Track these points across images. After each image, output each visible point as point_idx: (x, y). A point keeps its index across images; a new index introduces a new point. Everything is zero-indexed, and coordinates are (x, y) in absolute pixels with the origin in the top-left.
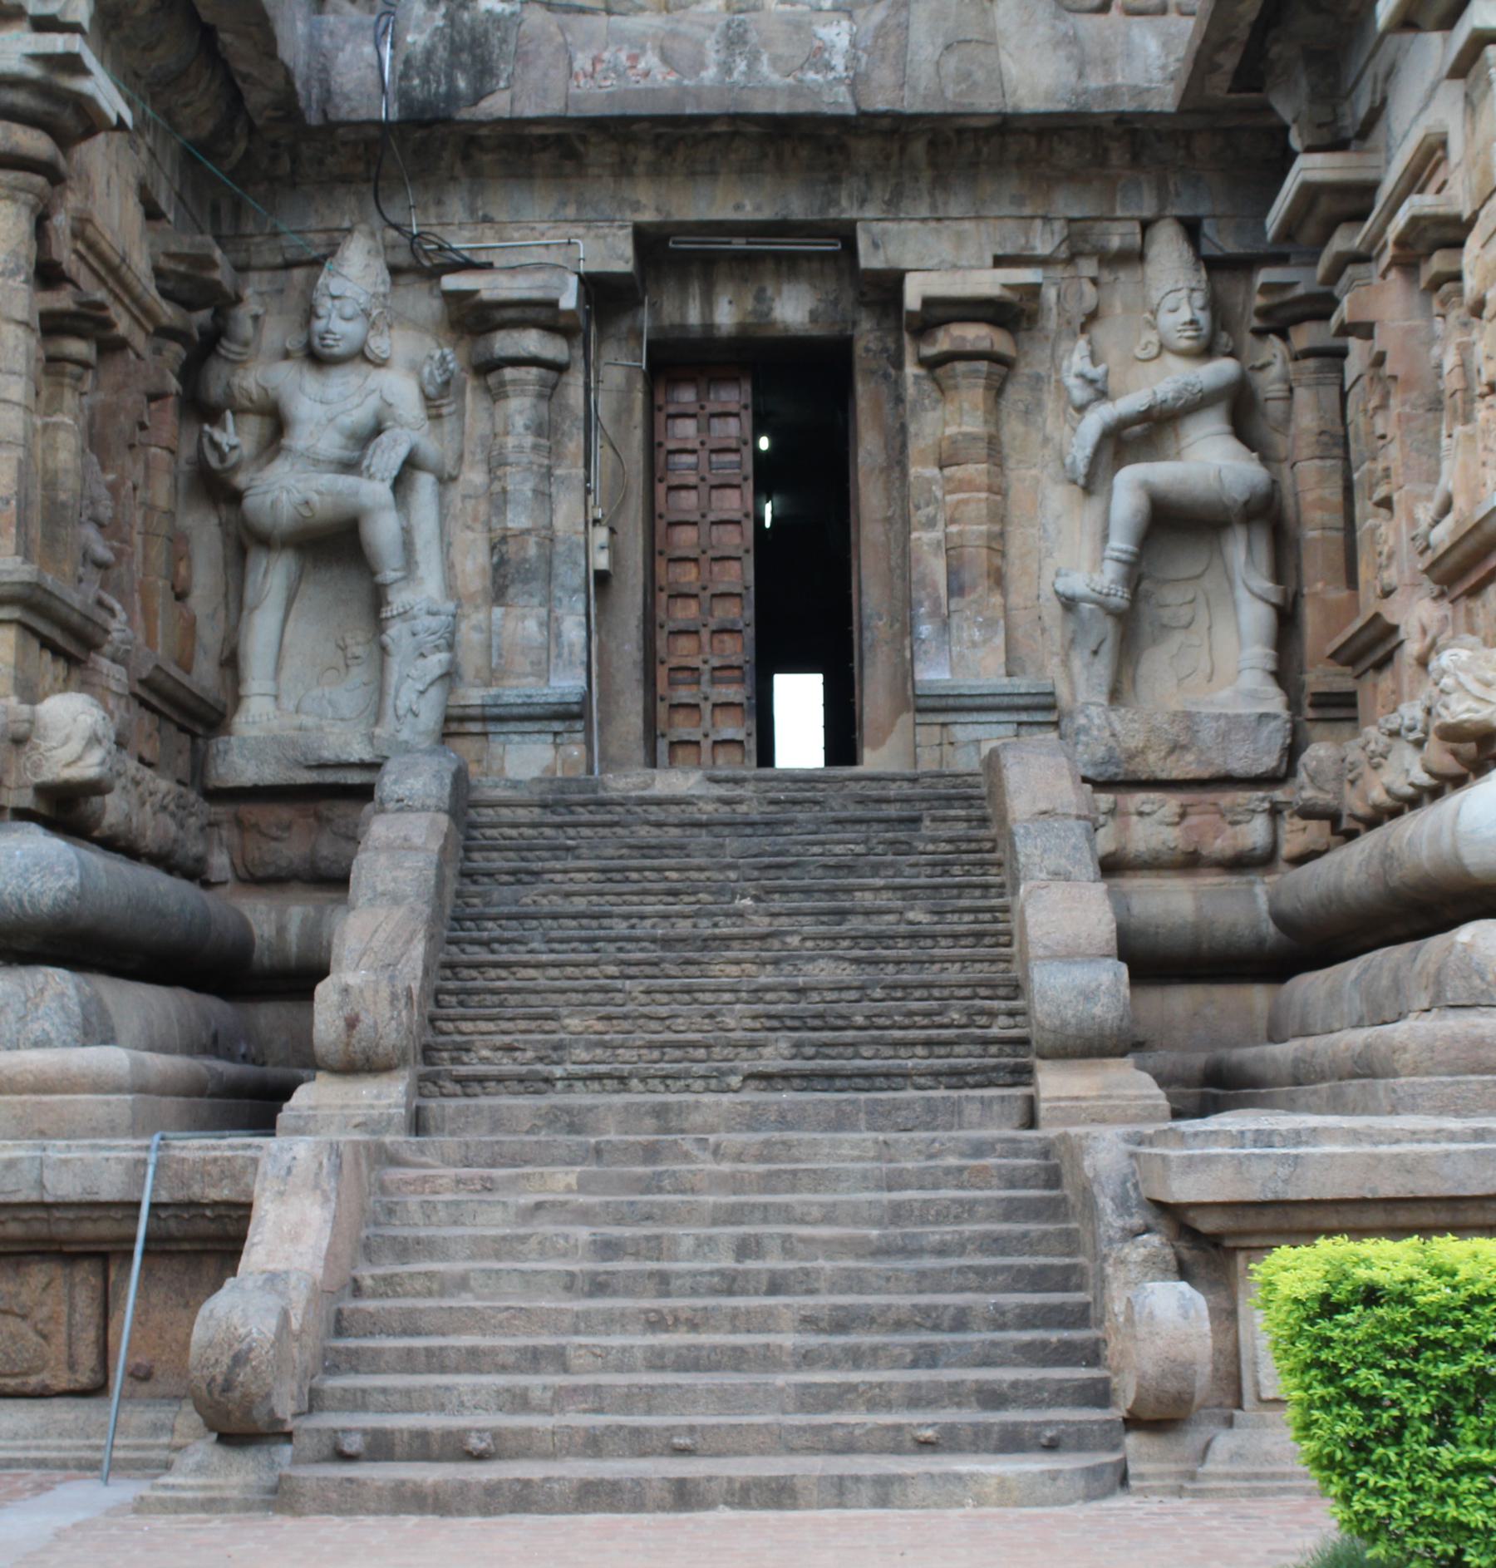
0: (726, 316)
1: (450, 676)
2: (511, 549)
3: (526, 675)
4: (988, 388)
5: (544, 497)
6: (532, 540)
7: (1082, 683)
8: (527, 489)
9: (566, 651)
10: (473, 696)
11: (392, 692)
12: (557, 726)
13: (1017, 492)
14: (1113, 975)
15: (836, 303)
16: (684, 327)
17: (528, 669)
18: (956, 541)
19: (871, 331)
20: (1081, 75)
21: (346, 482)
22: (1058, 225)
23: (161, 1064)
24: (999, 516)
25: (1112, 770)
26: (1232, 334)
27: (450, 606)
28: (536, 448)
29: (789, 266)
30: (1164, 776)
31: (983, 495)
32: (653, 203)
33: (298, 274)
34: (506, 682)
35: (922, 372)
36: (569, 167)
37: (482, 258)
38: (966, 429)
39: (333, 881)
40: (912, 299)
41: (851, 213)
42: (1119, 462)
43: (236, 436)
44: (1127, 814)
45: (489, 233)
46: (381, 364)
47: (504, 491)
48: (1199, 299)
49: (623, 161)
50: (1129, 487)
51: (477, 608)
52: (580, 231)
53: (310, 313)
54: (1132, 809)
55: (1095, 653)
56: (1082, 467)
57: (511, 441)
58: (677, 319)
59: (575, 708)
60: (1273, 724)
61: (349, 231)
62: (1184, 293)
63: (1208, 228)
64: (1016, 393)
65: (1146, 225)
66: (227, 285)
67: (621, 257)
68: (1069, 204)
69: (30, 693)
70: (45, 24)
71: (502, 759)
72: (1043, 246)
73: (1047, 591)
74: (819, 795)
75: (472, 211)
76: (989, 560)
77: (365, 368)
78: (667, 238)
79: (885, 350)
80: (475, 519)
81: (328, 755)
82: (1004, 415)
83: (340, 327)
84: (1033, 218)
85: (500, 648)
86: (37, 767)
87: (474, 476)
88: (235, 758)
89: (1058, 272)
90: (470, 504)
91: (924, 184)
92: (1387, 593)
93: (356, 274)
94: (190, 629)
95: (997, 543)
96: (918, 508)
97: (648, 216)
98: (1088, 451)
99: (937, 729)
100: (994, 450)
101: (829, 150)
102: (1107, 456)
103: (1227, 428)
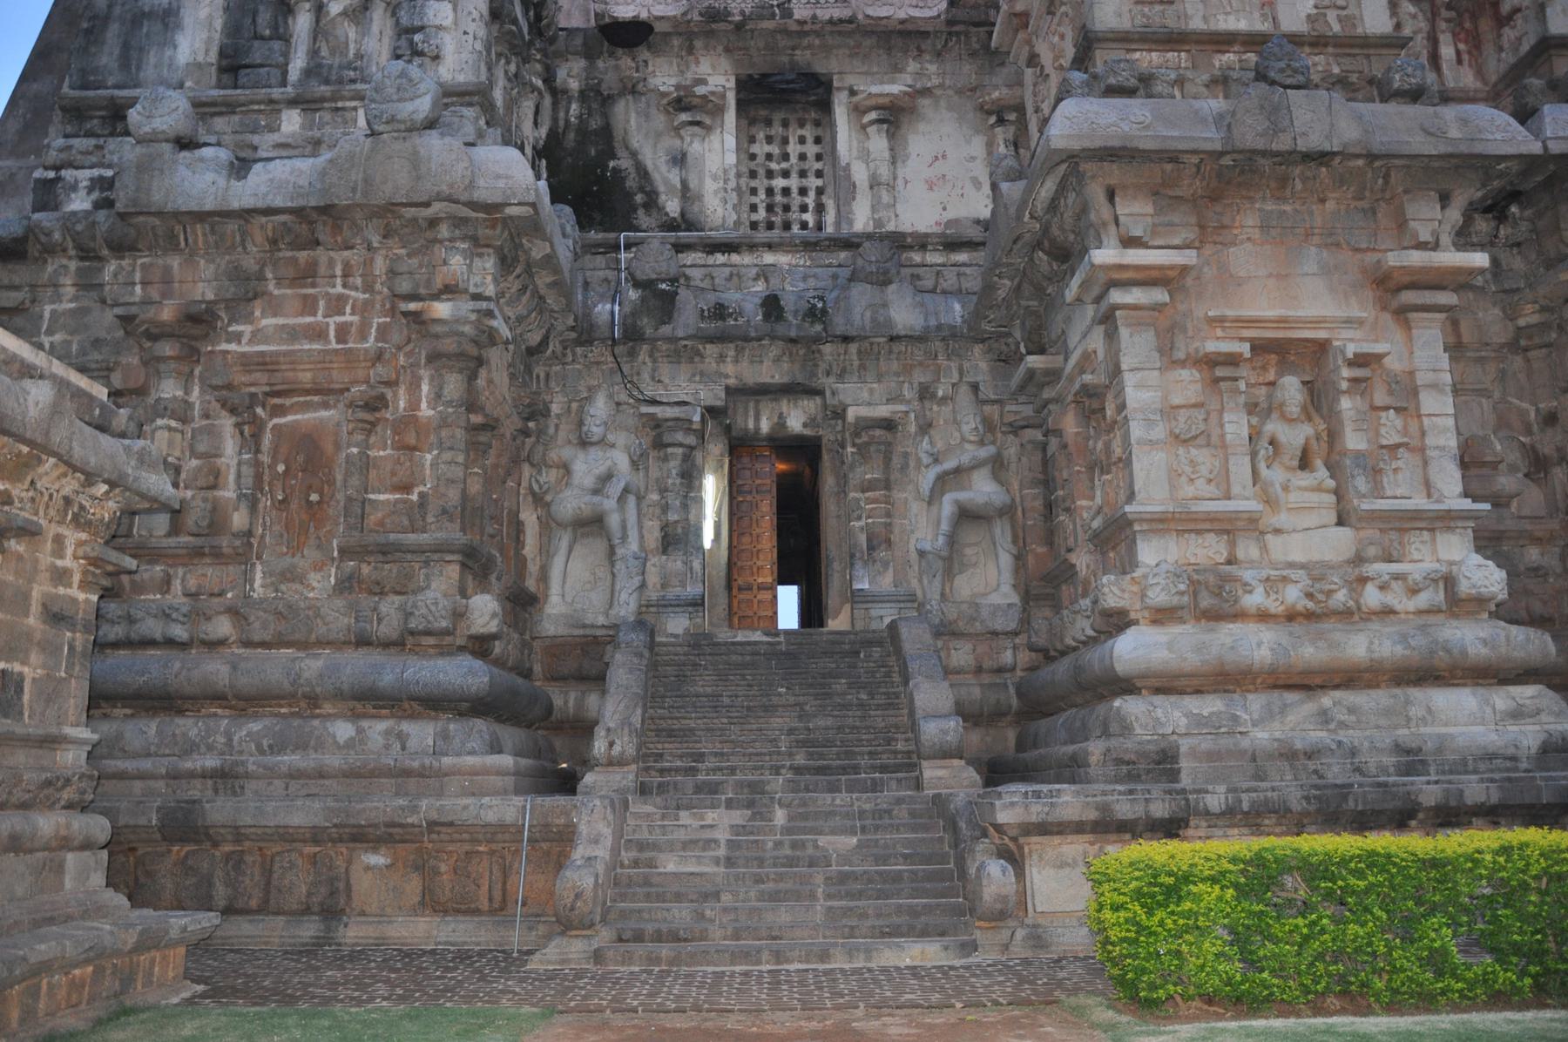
1: (643, 585)
2: (670, 530)
14: (953, 724)
21: (597, 499)
23: (525, 762)
36: (697, 359)
39: (599, 679)
43: (550, 476)
46: (613, 446)
53: (581, 423)
56: (927, 493)
69: (464, 594)
70: (477, 297)
73: (912, 548)
83: (596, 431)
86: (469, 627)
92: (1069, 550)
97: (732, 381)
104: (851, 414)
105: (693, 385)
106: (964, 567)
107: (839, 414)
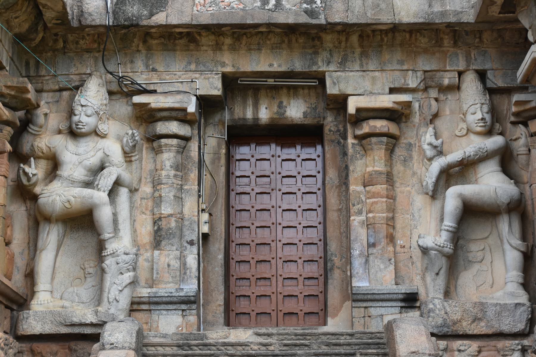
0: (265, 114)
1: (134, 283)
2: (163, 224)
3: (170, 283)
4: (386, 150)
5: (179, 199)
6: (173, 219)
7: (431, 289)
8: (171, 195)
9: (188, 271)
10: (144, 292)
11: (107, 290)
12: (184, 307)
13: (400, 198)
15: (315, 109)
16: (245, 119)
17: (171, 280)
18: (372, 221)
19: (332, 122)
20: (430, 6)
21: (87, 192)
22: (419, 74)
24: (392, 209)
25: (446, 329)
26: (501, 124)
27: (134, 250)
28: (175, 176)
29: (293, 91)
30: (470, 332)
31: (385, 200)
32: (232, 62)
33: (66, 94)
34: (160, 286)
35: (356, 142)
36: (192, 46)
37: (152, 88)
38: (376, 169)
40: (351, 109)
41: (323, 68)
42: (448, 186)
43: (35, 170)
44: (453, 351)
45: (155, 76)
46: (103, 136)
47: (160, 196)
48: (486, 108)
49: (217, 44)
50: (453, 197)
51: (147, 250)
52: (197, 76)
53: (71, 113)
54: (455, 348)
55: (437, 274)
56: (431, 187)
57: (164, 173)
58: (241, 116)
59: (192, 299)
60: (522, 309)
61: (90, 75)
62: (479, 105)
63: (489, 74)
64: (400, 152)
65: (460, 74)
66: (33, 100)
67: (216, 88)
68: (425, 64)
71: (158, 322)
72: (412, 84)
73: (414, 244)
74: (307, 342)
75: (147, 66)
76: (387, 230)
77: (96, 138)
78: (237, 79)
79: (338, 131)
80: (146, 209)
81: (76, 320)
82: (394, 162)
83: (85, 120)
84: (408, 70)
85: (157, 270)
87: (146, 189)
88: (31, 320)
89: (419, 95)
90: (144, 202)
91: (357, 55)
93: (93, 94)
94: (11, 259)
95: (391, 222)
96: (354, 205)
97: (228, 69)
98: (434, 179)
99: (363, 309)
100: (390, 178)
101: (313, 39)
102: (442, 182)
103: (499, 169)
104: (352, 106)
105: (190, 74)
106: (470, 263)
107: (339, 103)
